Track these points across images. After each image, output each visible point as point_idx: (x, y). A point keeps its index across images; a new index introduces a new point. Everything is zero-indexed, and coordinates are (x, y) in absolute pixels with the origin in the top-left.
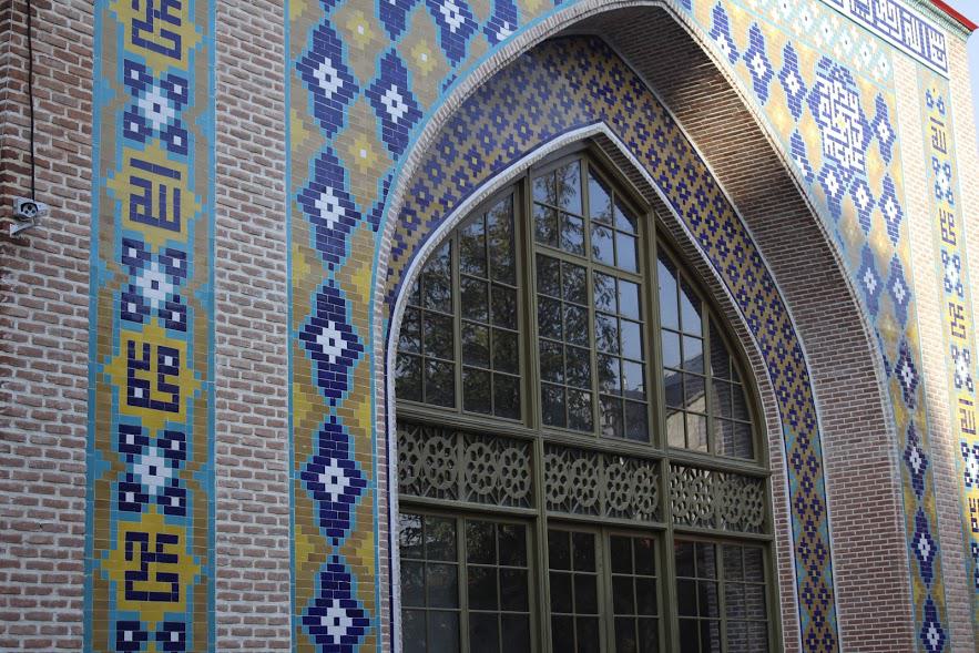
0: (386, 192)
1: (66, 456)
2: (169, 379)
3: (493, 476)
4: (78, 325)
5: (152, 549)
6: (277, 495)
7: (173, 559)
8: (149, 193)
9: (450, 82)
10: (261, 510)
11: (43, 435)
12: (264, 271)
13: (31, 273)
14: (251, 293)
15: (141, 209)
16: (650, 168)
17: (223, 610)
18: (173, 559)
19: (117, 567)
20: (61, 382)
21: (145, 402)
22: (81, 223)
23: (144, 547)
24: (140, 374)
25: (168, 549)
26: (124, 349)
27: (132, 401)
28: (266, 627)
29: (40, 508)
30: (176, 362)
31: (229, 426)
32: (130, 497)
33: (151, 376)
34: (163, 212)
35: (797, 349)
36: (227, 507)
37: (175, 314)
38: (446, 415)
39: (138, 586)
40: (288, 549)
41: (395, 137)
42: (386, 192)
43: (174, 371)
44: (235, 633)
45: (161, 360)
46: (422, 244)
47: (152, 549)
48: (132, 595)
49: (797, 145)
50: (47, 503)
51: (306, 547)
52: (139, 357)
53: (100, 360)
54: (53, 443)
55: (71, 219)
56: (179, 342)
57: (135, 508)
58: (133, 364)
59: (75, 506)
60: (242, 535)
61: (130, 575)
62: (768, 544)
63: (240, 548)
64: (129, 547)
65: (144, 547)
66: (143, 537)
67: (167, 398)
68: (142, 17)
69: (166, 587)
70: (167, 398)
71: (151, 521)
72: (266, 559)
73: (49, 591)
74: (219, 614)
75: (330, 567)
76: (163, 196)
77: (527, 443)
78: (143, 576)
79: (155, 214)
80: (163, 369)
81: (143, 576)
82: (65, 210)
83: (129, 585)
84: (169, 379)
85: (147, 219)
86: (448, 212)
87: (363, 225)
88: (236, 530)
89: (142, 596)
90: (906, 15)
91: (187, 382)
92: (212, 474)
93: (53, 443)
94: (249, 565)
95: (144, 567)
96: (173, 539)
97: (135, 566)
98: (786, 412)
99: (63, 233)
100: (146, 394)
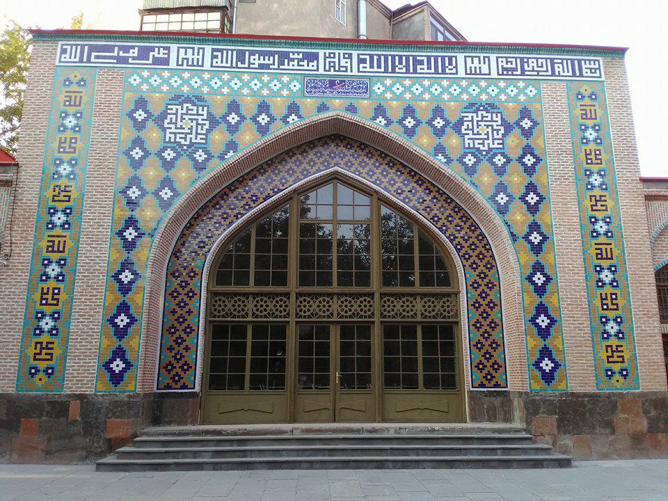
0: (158, 223)
1: (16, 322)
2: (55, 297)
3: (268, 309)
4: (24, 285)
5: (44, 346)
6: (96, 327)
7: (52, 349)
8: (54, 244)
9: (196, 180)
10: (88, 332)
11: (9, 317)
12: (98, 259)
13: (10, 273)
14: (91, 266)
15: (50, 249)
16: (368, 178)
17: (69, 363)
18: (52, 349)
19: (31, 352)
20: (16, 302)
21: (46, 304)
22: (28, 256)
23: (41, 346)
24: (45, 296)
25: (50, 346)
26: (40, 290)
27: (41, 304)
28: (86, 368)
29: (6, 336)
30: (59, 291)
31: (77, 307)
32: (38, 332)
33: (49, 296)
34: (58, 249)
35: (482, 234)
36: (74, 332)
37: (60, 278)
38: (247, 289)
39: (38, 357)
40: (98, 344)
41: (165, 205)
42: (158, 223)
43: (58, 294)
44: (73, 370)
45: (54, 291)
46: (222, 233)
47: (44, 346)
48: (35, 359)
49: (439, 149)
50: (8, 335)
51: (106, 342)
52: (45, 291)
53: (31, 294)
54: (12, 319)
55: (24, 256)
56: (61, 285)
57: (39, 335)
58: (43, 293)
59: (19, 335)
60: (79, 340)
61: (35, 354)
62: (457, 323)
63: (78, 345)
64: (36, 346)
65: (41, 346)
66: (41, 343)
67: (55, 302)
68: (56, 193)
69: (49, 357)
70: (55, 302)
71: (45, 338)
72: (89, 347)
73: (7, 359)
74: (67, 364)
75: (116, 348)
76: (59, 244)
77: (287, 295)
78: (40, 354)
79: (56, 249)
80: (54, 294)
81: (40, 354)
82: (22, 254)
83: (35, 357)
84: (55, 297)
85: (53, 251)
86: (237, 218)
87: (145, 239)
88: (77, 339)
89: (40, 360)
90: (555, 61)
91: (63, 297)
92: (70, 323)
93: (12, 319)
94: (81, 349)
95: (41, 352)
96: (53, 343)
97: (38, 351)
98: (467, 264)
99: (21, 261)
100: (47, 302)
